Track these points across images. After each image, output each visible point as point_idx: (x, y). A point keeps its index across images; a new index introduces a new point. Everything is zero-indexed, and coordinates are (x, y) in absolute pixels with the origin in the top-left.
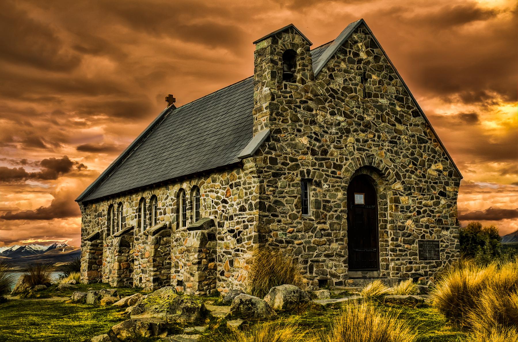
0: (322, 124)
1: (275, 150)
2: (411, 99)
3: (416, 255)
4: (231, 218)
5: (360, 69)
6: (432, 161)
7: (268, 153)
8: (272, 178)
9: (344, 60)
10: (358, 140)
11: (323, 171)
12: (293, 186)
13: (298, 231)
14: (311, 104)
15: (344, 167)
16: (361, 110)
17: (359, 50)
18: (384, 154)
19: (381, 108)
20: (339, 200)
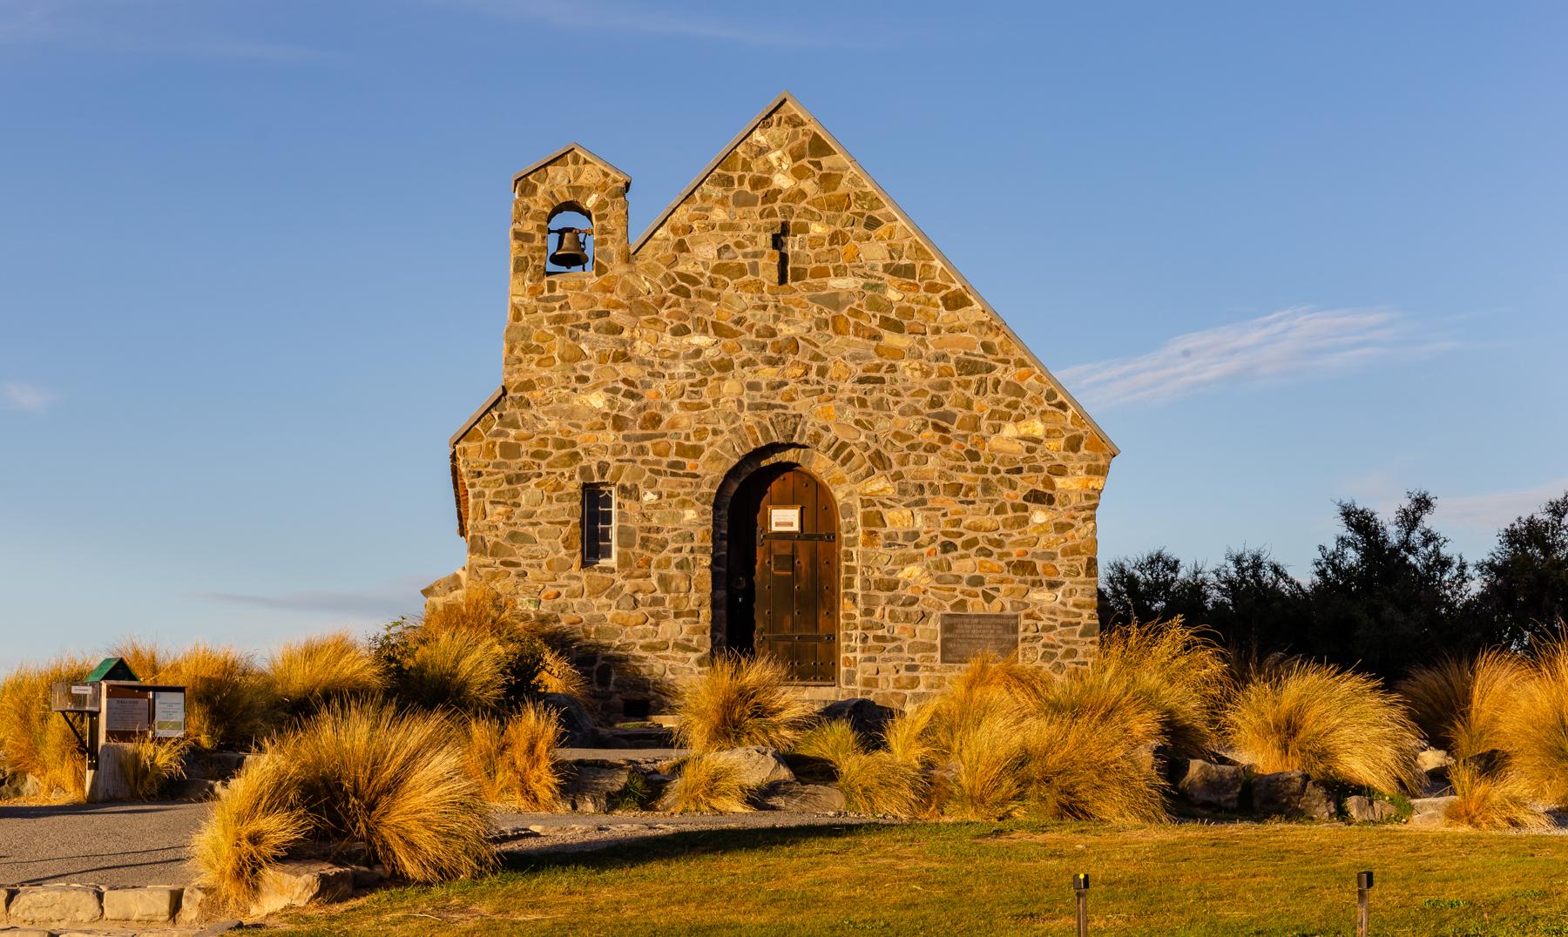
0: (649, 358)
1: (518, 427)
2: (938, 263)
3: (933, 648)
5: (772, 213)
6: (1005, 417)
7: (498, 434)
8: (505, 486)
9: (722, 202)
10: (753, 386)
11: (644, 462)
12: (559, 500)
13: (572, 595)
14: (617, 316)
15: (707, 453)
16: (771, 312)
17: (771, 169)
18: (833, 412)
19: (834, 301)
20: (690, 523)
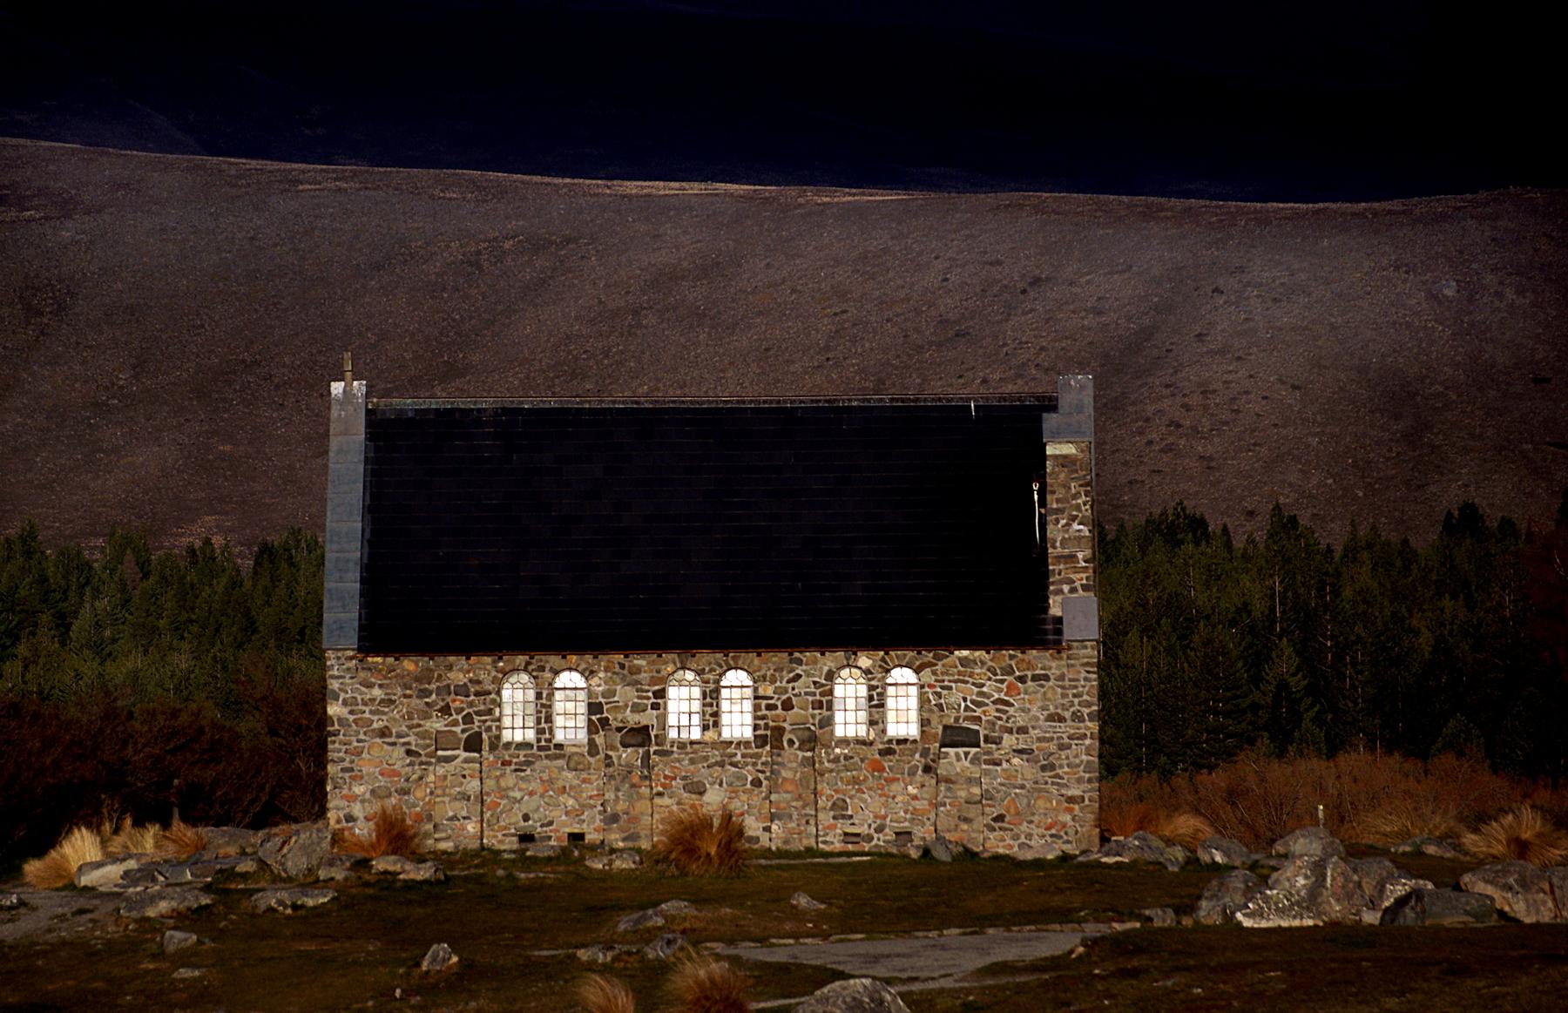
4: (1023, 730)
